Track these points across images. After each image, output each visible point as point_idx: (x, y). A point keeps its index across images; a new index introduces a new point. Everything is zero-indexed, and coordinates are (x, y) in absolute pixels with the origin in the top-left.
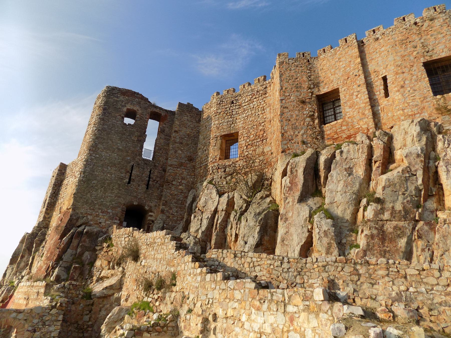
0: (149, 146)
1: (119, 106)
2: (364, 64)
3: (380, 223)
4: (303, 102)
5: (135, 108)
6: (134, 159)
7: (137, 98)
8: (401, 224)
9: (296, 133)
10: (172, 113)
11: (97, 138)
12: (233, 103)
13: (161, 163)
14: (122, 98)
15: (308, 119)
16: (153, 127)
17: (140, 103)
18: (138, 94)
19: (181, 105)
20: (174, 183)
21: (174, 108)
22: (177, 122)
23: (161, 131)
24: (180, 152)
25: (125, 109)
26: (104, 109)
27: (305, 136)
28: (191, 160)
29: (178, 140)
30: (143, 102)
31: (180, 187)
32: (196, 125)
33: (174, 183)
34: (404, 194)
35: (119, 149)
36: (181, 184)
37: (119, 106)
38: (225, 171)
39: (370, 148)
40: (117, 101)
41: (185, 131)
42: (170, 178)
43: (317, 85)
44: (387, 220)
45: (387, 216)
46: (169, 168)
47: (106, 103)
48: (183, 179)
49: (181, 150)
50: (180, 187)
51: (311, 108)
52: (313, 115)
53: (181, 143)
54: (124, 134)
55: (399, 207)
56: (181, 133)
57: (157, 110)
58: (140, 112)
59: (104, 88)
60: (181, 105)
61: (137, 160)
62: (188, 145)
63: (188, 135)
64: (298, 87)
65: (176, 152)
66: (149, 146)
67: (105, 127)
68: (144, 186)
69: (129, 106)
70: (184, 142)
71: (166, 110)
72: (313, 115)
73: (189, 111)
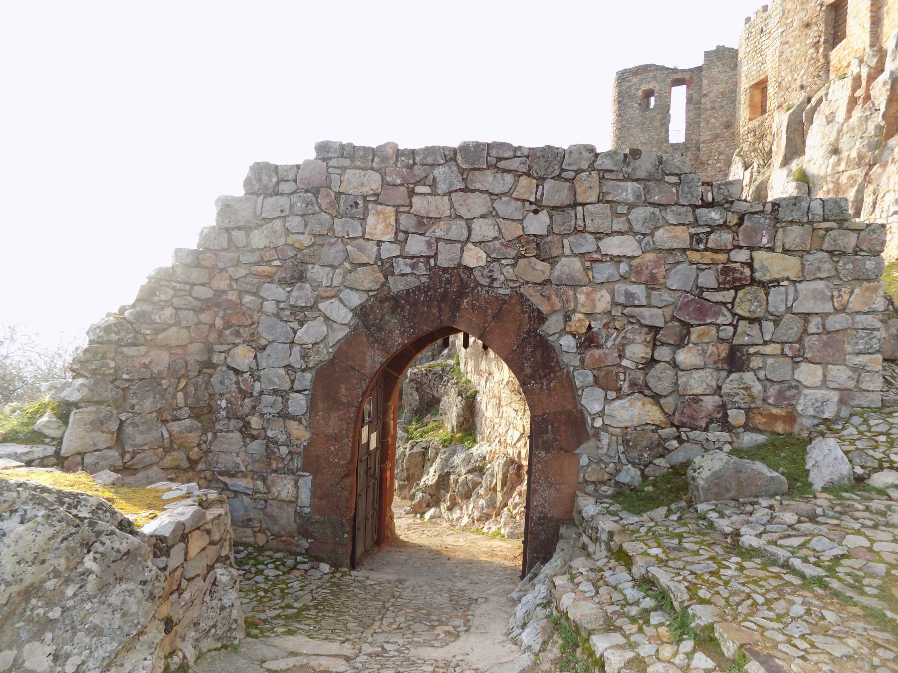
1: (633, 91)
3: (837, 175)
4: (808, 25)
5: (651, 87)
6: (660, 149)
7: (651, 71)
8: (855, 172)
9: (795, 76)
10: (699, 69)
11: (619, 139)
12: (762, 31)
13: (694, 142)
14: (634, 80)
15: (812, 51)
17: (655, 77)
18: (651, 65)
20: (709, 162)
21: (699, 62)
22: (705, 82)
23: (689, 100)
24: (714, 121)
25: (640, 93)
26: (619, 102)
27: (805, 77)
28: (728, 126)
29: (709, 106)
30: (659, 73)
31: (718, 165)
32: (731, 74)
33: (709, 162)
34: (861, 138)
35: (642, 143)
36: (718, 161)
37: (633, 91)
38: (755, 135)
39: (857, 81)
40: (630, 87)
41: (717, 89)
42: (705, 158)
44: (843, 172)
45: (842, 167)
46: (701, 146)
47: (620, 94)
48: (720, 154)
49: (715, 118)
50: (718, 165)
52: (818, 42)
53: (714, 108)
54: (644, 123)
55: (854, 154)
56: (712, 95)
57: (678, 76)
58: (657, 89)
59: (615, 76)
61: (663, 148)
62: (723, 107)
63: (722, 93)
65: (708, 122)
67: (624, 122)
69: (644, 87)
70: (717, 105)
71: (690, 70)
72: (818, 42)
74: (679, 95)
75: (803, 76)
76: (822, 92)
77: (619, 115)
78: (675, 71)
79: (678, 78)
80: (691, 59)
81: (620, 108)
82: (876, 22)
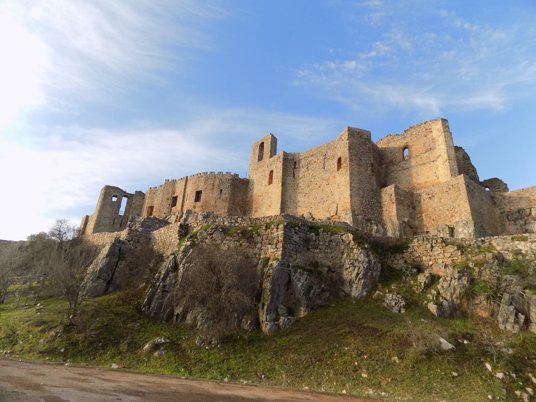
0: (122, 211)
2: (185, 189)
10: (133, 195)
14: (112, 190)
16: (124, 200)
19: (136, 191)
21: (133, 192)
22: (134, 200)
23: (128, 203)
39: (177, 216)
43: (174, 193)
47: (105, 193)
51: (170, 202)
60: (136, 191)
64: (168, 193)
66: (122, 211)
68: (119, 226)
69: (114, 194)
73: (140, 194)
74: (124, 200)
75: (165, 210)
76: (169, 216)
77: (103, 200)
78: (125, 192)
79: (126, 195)
80: (131, 191)
81: (104, 198)
82: (182, 206)
